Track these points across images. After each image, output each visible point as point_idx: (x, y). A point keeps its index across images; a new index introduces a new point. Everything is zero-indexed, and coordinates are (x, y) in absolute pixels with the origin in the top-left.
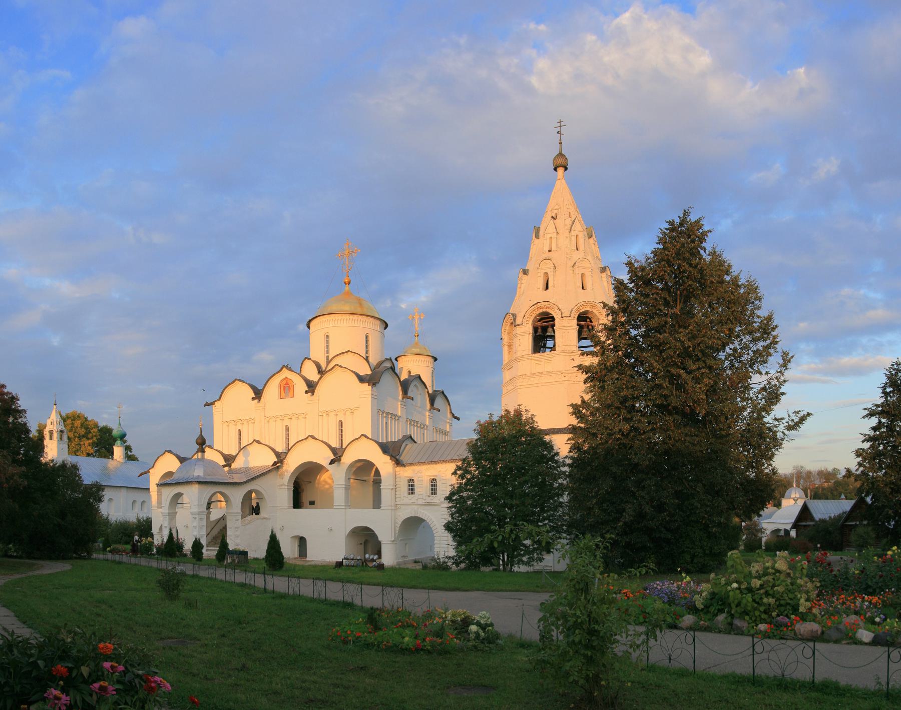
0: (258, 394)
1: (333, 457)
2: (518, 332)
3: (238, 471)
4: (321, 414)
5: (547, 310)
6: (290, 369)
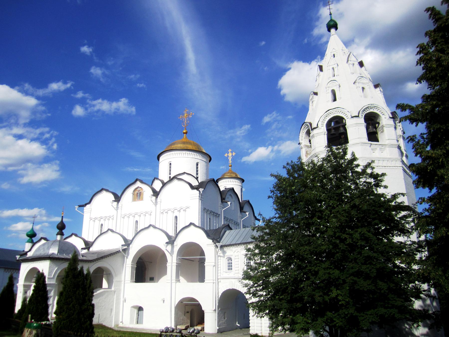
0: (118, 198)
3: (94, 253)
4: (162, 212)
6: (142, 182)
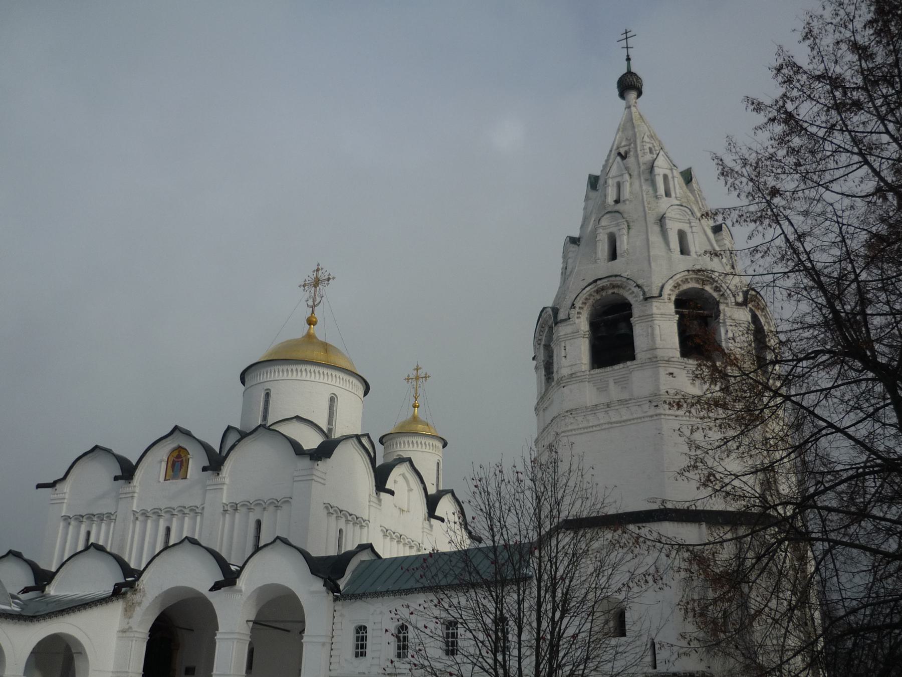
1: (220, 578)
2: (561, 334)
5: (616, 290)
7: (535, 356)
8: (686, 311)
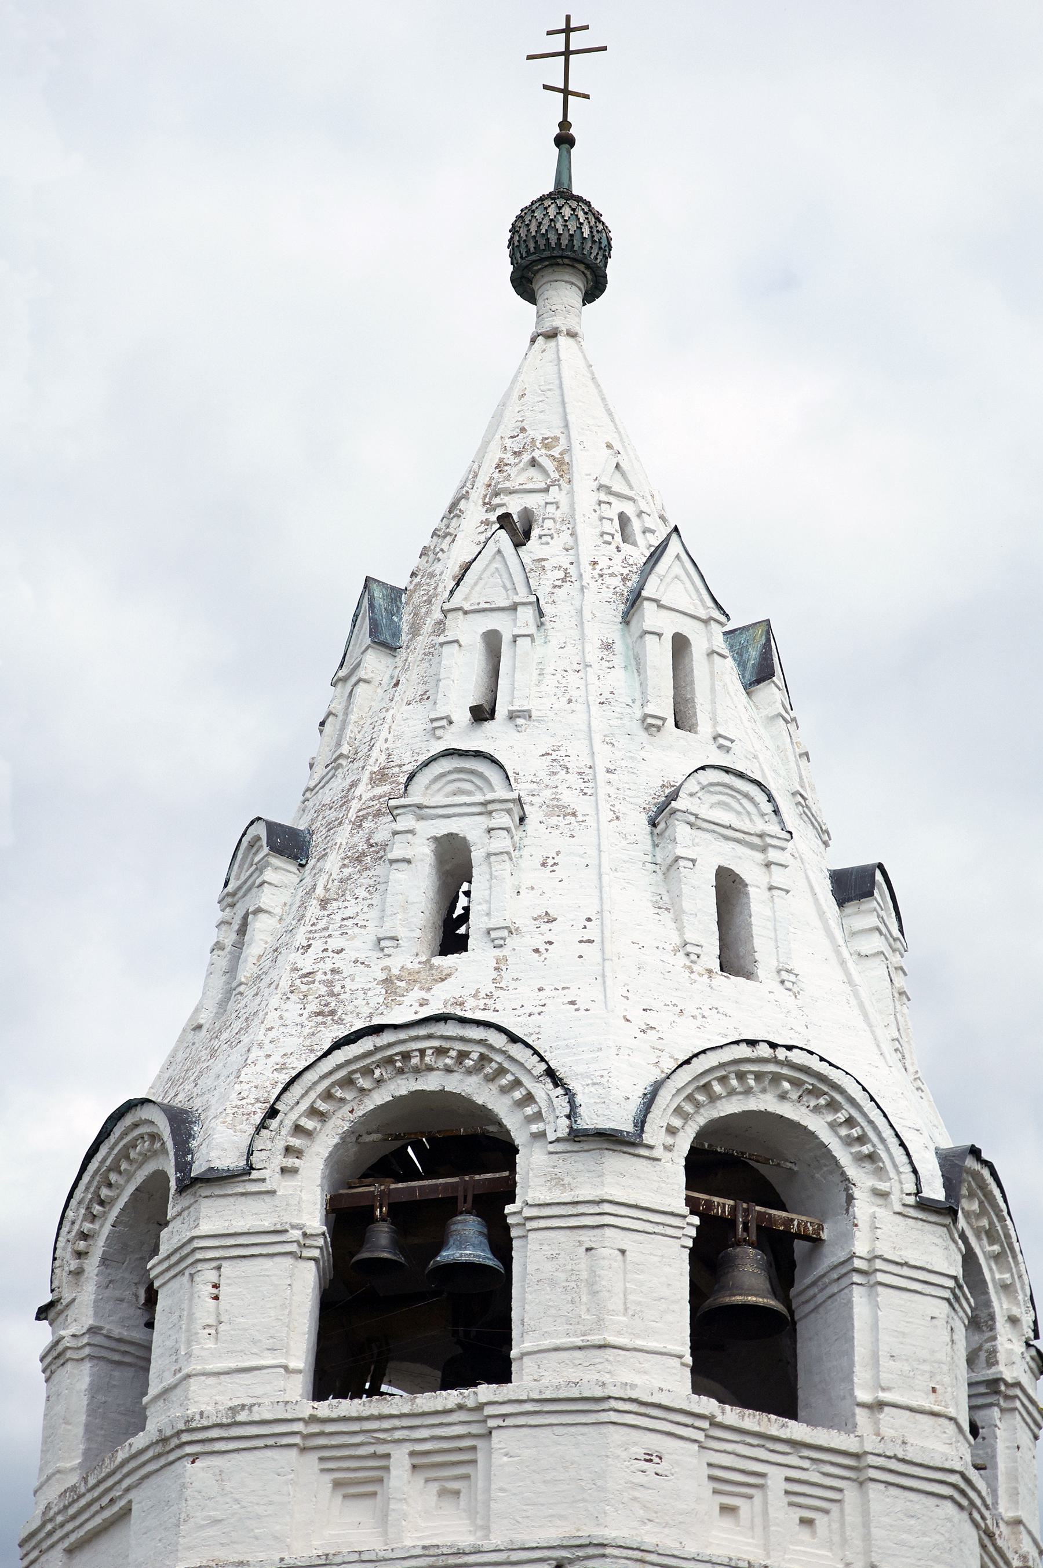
7: (51, 1305)
8: (722, 1205)
